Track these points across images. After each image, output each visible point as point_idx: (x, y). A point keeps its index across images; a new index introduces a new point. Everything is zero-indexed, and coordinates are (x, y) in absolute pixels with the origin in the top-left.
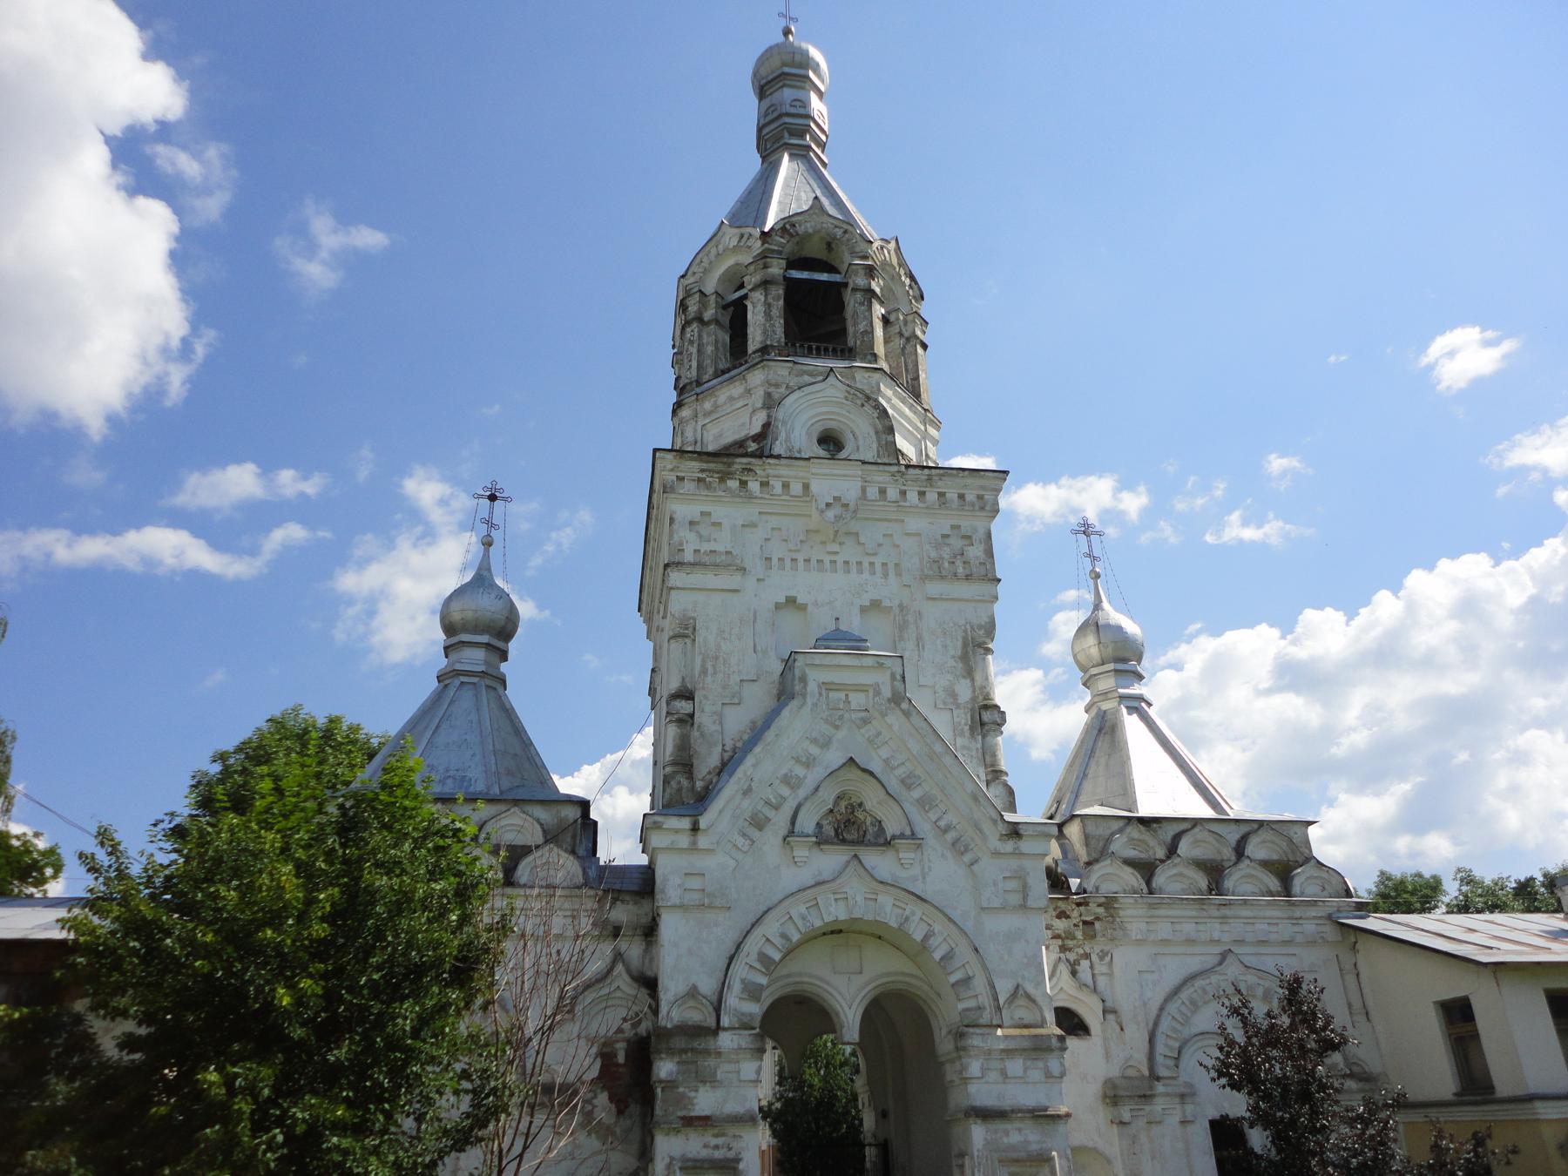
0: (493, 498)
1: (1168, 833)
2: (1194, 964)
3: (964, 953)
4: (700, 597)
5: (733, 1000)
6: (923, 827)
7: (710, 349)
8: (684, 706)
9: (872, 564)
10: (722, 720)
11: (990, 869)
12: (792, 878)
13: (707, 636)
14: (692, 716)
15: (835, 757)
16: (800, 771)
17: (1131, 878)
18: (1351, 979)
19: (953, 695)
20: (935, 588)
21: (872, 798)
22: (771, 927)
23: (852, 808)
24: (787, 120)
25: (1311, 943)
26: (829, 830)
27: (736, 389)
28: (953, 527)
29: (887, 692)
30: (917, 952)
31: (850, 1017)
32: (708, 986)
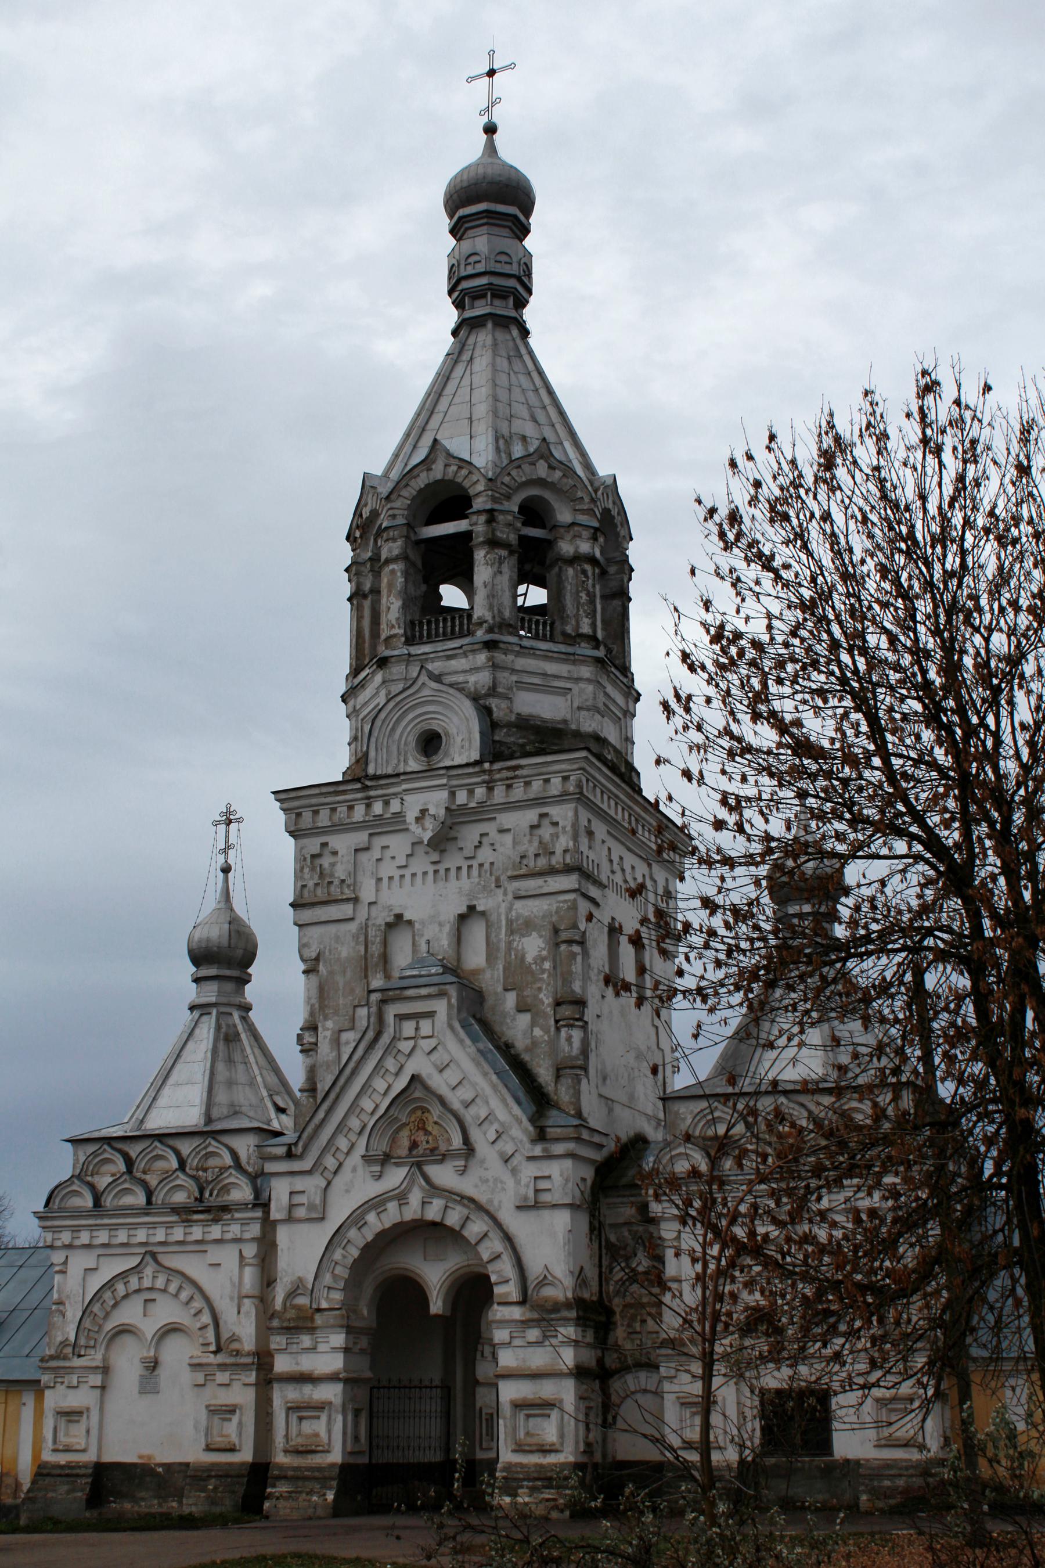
9: (470, 867)
14: (316, 1044)
28: (542, 816)
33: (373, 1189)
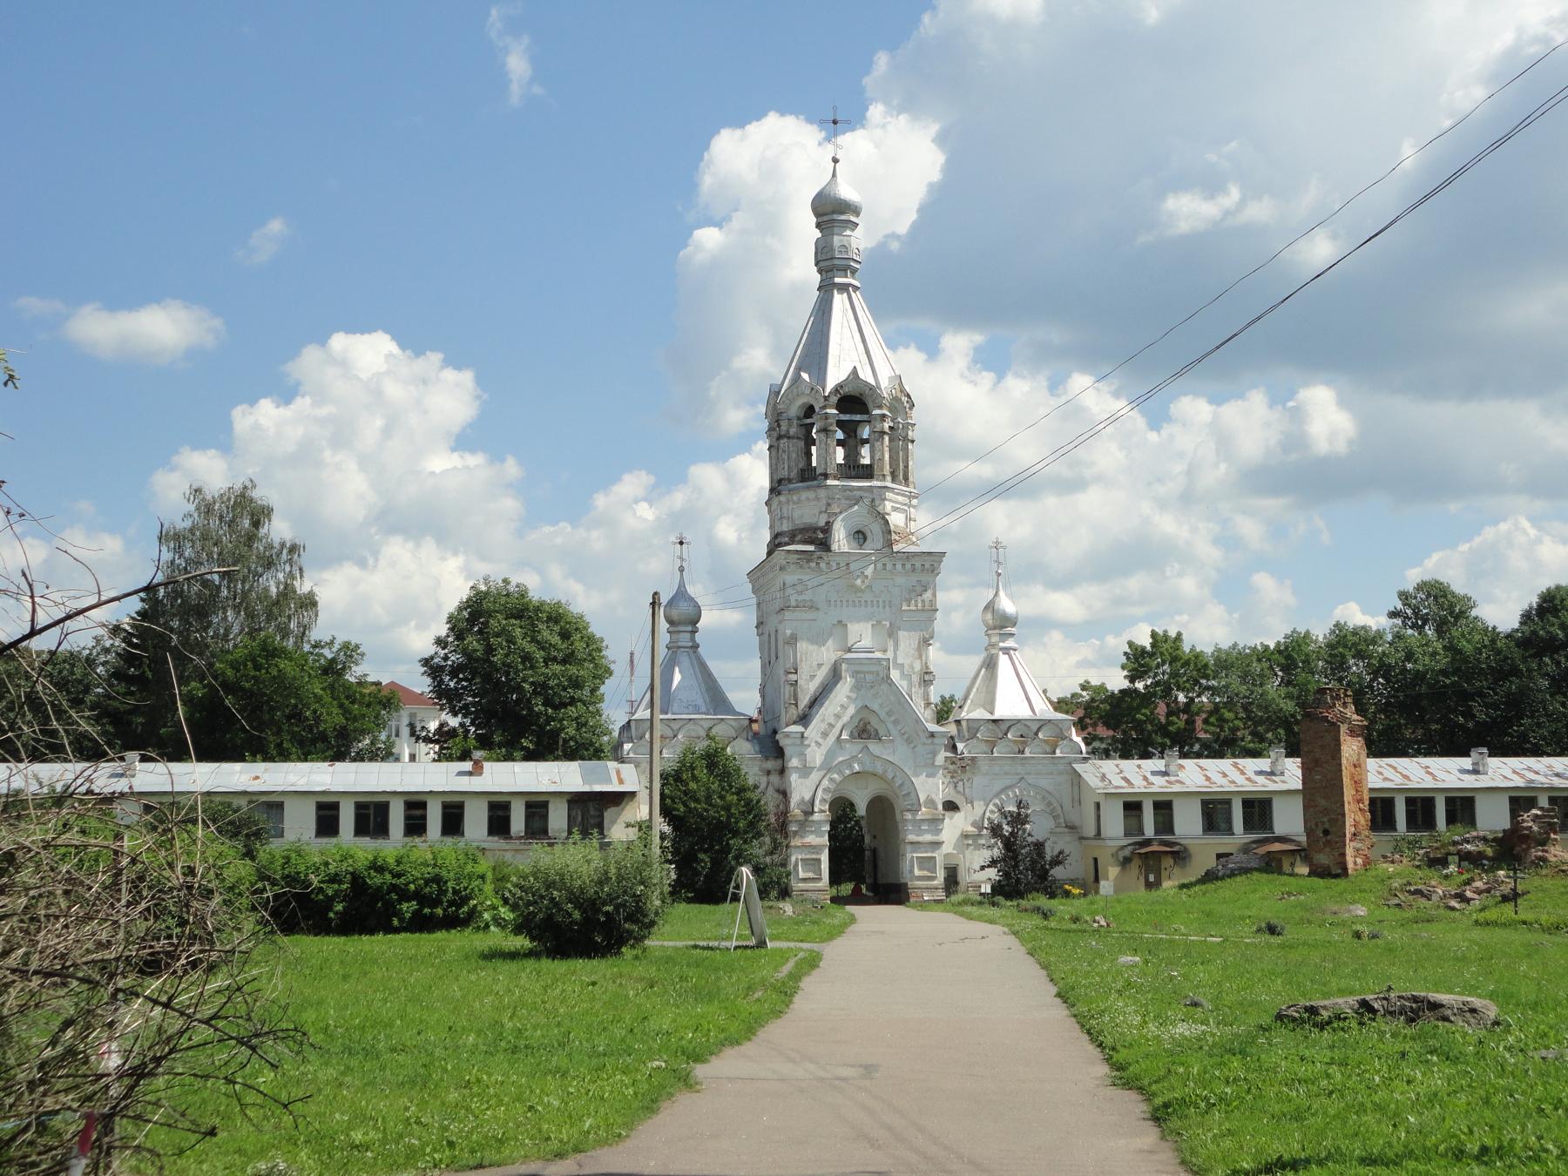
0: (681, 543)
1: (1004, 727)
2: (1008, 782)
5: (817, 802)
17: (984, 747)
21: (874, 722)
27: (811, 494)
30: (890, 783)
31: (861, 810)
32: (807, 797)
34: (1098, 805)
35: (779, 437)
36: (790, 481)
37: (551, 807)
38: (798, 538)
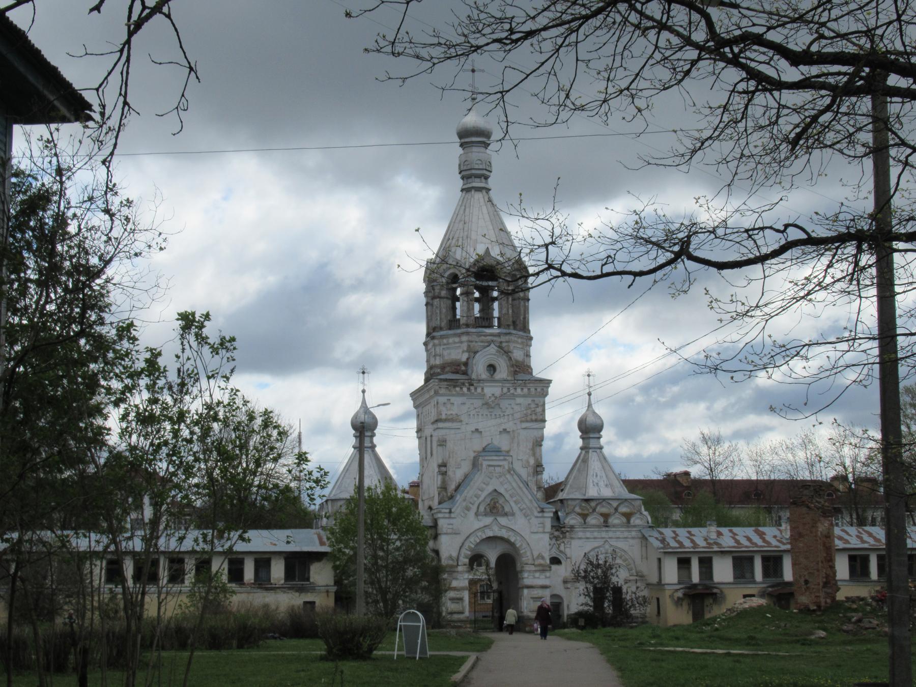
0: (363, 373)
2: (596, 544)
3: (524, 545)
4: (447, 431)
6: (515, 508)
7: (444, 310)
8: (443, 469)
10: (456, 475)
11: (534, 521)
12: (478, 525)
13: (450, 444)
15: (490, 489)
16: (480, 493)
17: (580, 519)
18: (644, 548)
19: (528, 462)
20: (525, 425)
22: (472, 539)
23: (495, 503)
24: (474, 172)
25: (633, 538)
26: (488, 510)
27: (457, 340)
29: (507, 467)
30: (512, 544)
32: (455, 554)
33: (481, 524)
34: (659, 560)
35: (434, 298)
36: (441, 329)
37: (273, 563)
38: (448, 369)
